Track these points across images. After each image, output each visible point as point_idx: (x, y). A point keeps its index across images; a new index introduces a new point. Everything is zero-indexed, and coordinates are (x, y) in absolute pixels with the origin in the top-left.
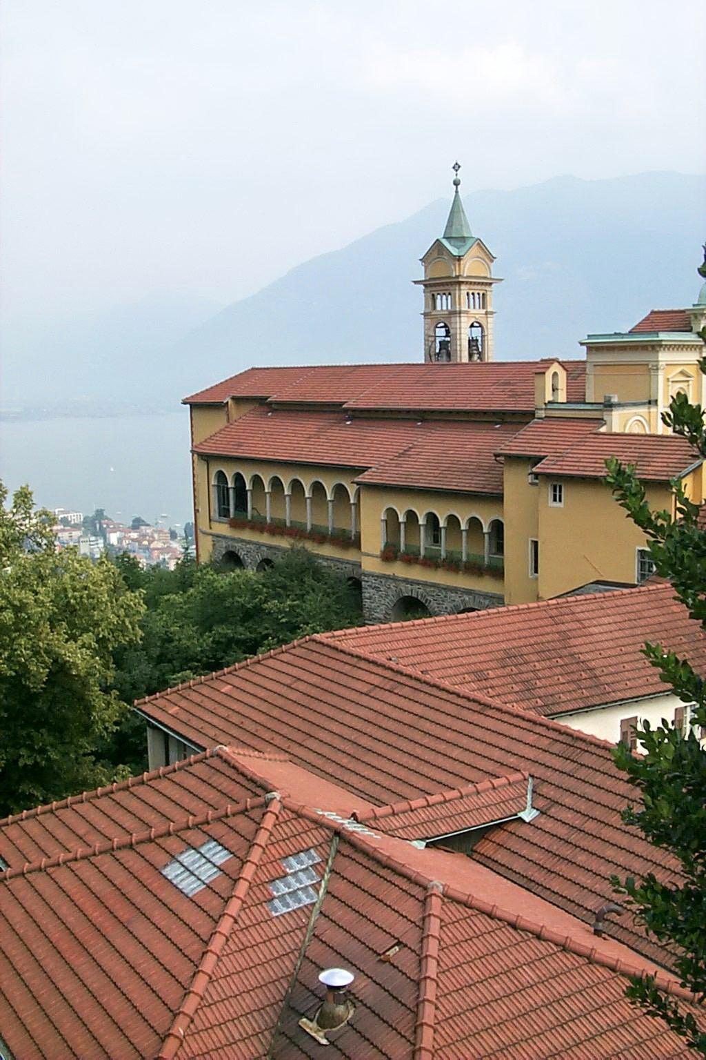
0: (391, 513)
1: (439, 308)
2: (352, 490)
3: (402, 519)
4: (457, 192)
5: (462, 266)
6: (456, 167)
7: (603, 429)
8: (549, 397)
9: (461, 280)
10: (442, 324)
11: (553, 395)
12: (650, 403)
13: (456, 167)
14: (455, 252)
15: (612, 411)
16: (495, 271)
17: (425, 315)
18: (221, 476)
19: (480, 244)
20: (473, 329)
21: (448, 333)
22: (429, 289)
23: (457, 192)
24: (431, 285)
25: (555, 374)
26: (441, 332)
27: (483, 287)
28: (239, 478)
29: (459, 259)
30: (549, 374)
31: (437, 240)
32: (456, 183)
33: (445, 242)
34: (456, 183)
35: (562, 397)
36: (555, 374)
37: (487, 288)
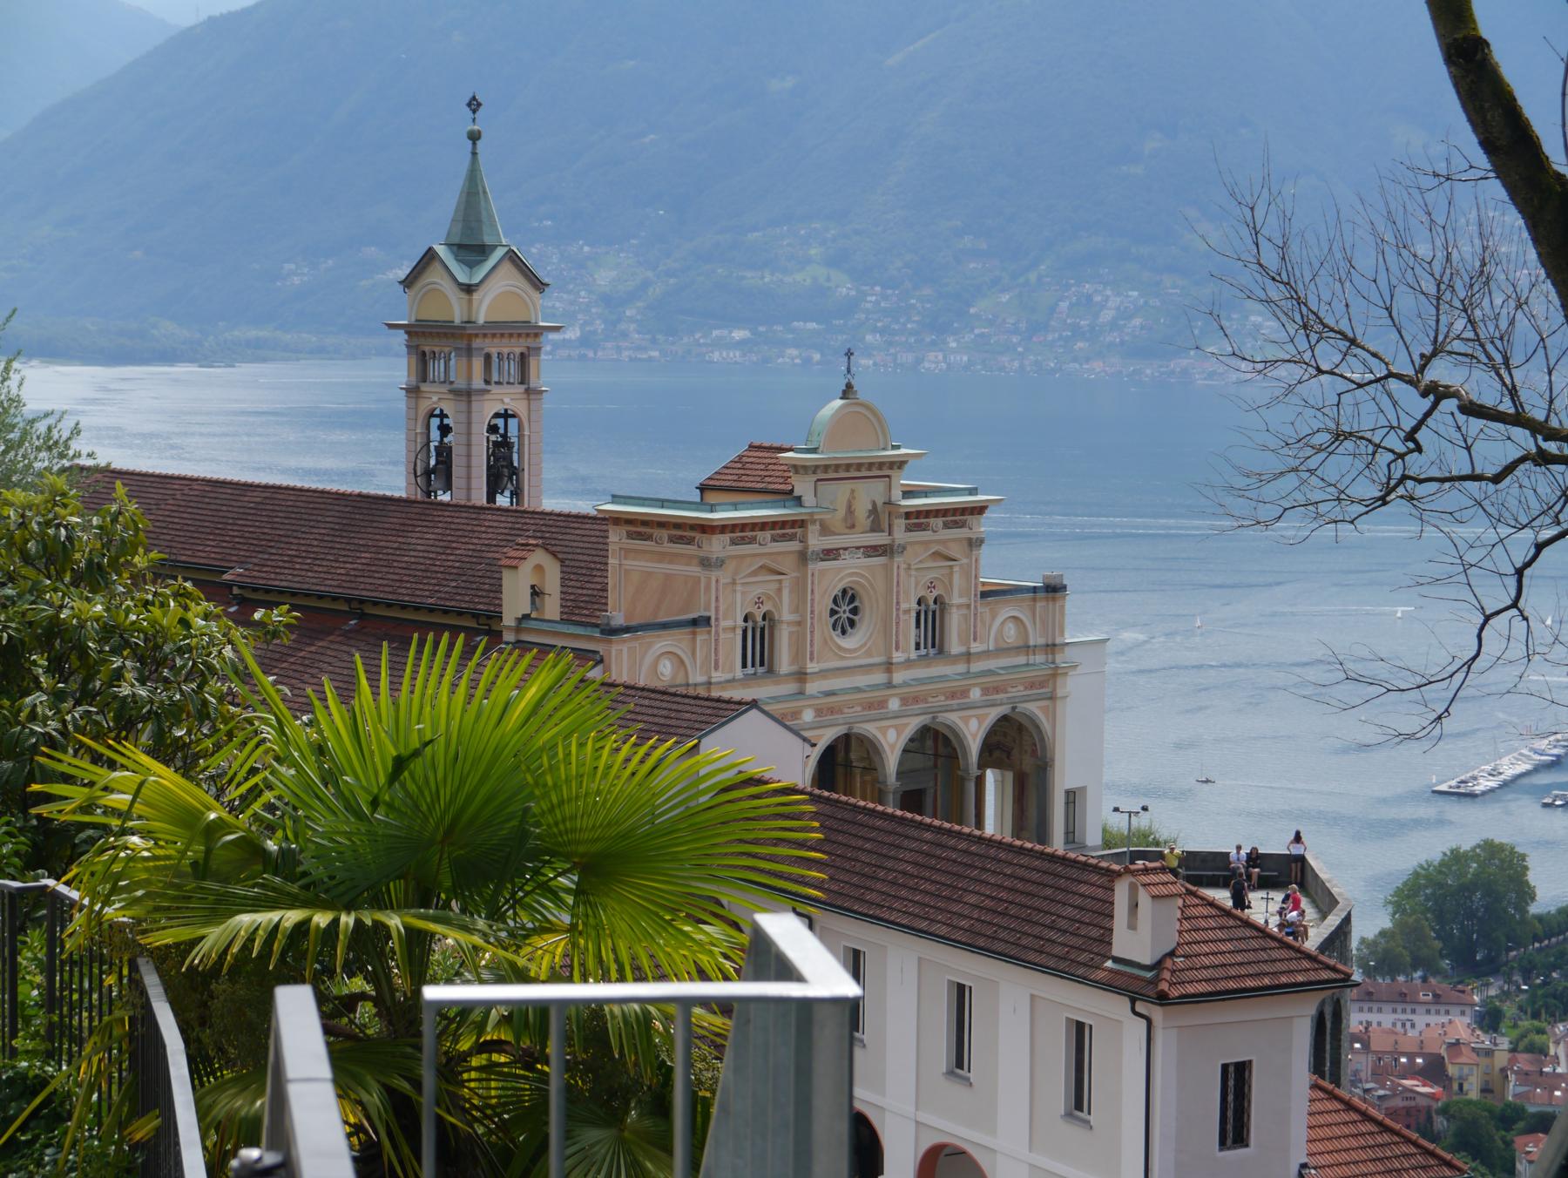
4: (474, 154)
5: (475, 304)
6: (474, 105)
11: (533, 602)
15: (610, 642)
16: (542, 309)
17: (408, 390)
19: (512, 257)
22: (415, 342)
23: (474, 154)
25: (539, 568)
29: (469, 289)
30: (526, 568)
31: (430, 249)
32: (474, 137)
34: (474, 137)
35: (552, 608)
36: (539, 568)
37: (530, 342)
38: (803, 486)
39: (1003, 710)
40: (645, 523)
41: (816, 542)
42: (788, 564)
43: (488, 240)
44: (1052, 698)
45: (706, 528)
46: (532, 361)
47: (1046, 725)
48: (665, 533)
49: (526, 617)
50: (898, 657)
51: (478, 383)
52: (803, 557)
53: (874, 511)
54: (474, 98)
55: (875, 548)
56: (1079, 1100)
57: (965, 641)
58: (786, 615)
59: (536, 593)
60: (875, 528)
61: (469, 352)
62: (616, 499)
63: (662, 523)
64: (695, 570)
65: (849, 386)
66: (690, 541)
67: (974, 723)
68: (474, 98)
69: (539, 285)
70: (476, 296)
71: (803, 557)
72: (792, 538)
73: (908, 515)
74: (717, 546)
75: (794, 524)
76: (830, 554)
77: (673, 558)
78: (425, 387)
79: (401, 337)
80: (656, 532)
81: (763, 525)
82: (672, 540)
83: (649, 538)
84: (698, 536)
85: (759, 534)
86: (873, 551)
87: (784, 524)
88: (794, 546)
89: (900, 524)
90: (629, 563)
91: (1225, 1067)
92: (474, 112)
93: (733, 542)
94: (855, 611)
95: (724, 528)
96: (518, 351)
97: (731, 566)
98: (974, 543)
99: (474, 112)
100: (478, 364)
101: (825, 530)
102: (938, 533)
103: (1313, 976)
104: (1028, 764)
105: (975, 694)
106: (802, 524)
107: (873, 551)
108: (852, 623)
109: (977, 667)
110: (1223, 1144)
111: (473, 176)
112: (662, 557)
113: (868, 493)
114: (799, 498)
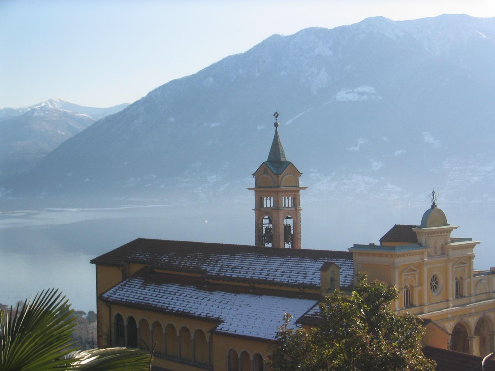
0: (233, 353)
1: (265, 206)
2: (208, 335)
3: (239, 357)
4: (276, 131)
6: (276, 115)
9: (279, 189)
10: (267, 217)
13: (276, 115)
18: (119, 317)
20: (287, 220)
21: (271, 222)
23: (276, 131)
24: (259, 191)
26: (266, 221)
27: (294, 194)
28: (131, 320)
32: (276, 125)
54: (276, 113)
68: (276, 113)
92: (276, 117)
99: (276, 117)
108: (436, 287)
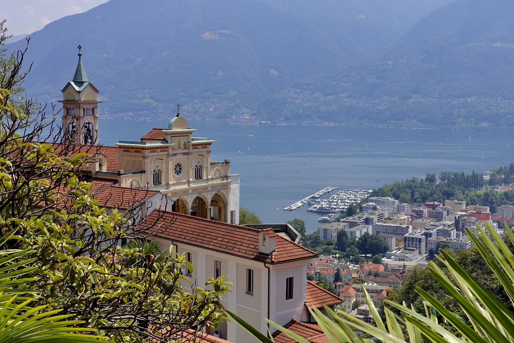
4: (80, 59)
6: (80, 48)
7: (117, 185)
8: (97, 169)
12: (141, 172)
13: (80, 48)
14: (77, 88)
19: (90, 85)
23: (80, 59)
29: (79, 92)
32: (80, 55)
33: (72, 83)
37: (95, 105)
38: (168, 138)
39: (216, 192)
40: (128, 148)
41: (171, 152)
42: (165, 156)
43: (84, 80)
44: (227, 189)
45: (144, 149)
46: (95, 110)
47: (226, 195)
48: (133, 150)
49: (98, 172)
50: (191, 180)
51: (82, 115)
52: (168, 155)
53: (185, 144)
55: (185, 153)
56: (250, 289)
57: (207, 176)
58: (164, 169)
59: (100, 165)
60: (185, 148)
61: (79, 108)
62: (120, 142)
63: (132, 148)
64: (141, 159)
65: (178, 114)
66: (140, 152)
67: (209, 196)
69: (97, 91)
70: (81, 94)
71: (168, 155)
72: (165, 151)
73: (193, 145)
74: (147, 153)
75: (166, 147)
76: (175, 155)
77: (135, 156)
78: (68, 116)
79: (62, 104)
80: (131, 150)
81: (158, 148)
82: (135, 152)
83: (129, 151)
84: (142, 150)
85: (157, 150)
86: (185, 154)
87: (163, 147)
88: (166, 153)
89: (191, 147)
90: (124, 158)
91: (287, 279)
93: (151, 152)
94: (180, 169)
95: (149, 148)
96: (92, 108)
97: (150, 158)
98: (209, 152)
100: (82, 110)
101: (173, 149)
102: (200, 150)
103: (308, 255)
104: (222, 205)
105: (210, 188)
106: (167, 147)
107: (185, 154)
108: (180, 172)
109: (210, 183)
110: (287, 299)
111: (79, 65)
112: (132, 156)
113: (183, 140)
114: (167, 141)
